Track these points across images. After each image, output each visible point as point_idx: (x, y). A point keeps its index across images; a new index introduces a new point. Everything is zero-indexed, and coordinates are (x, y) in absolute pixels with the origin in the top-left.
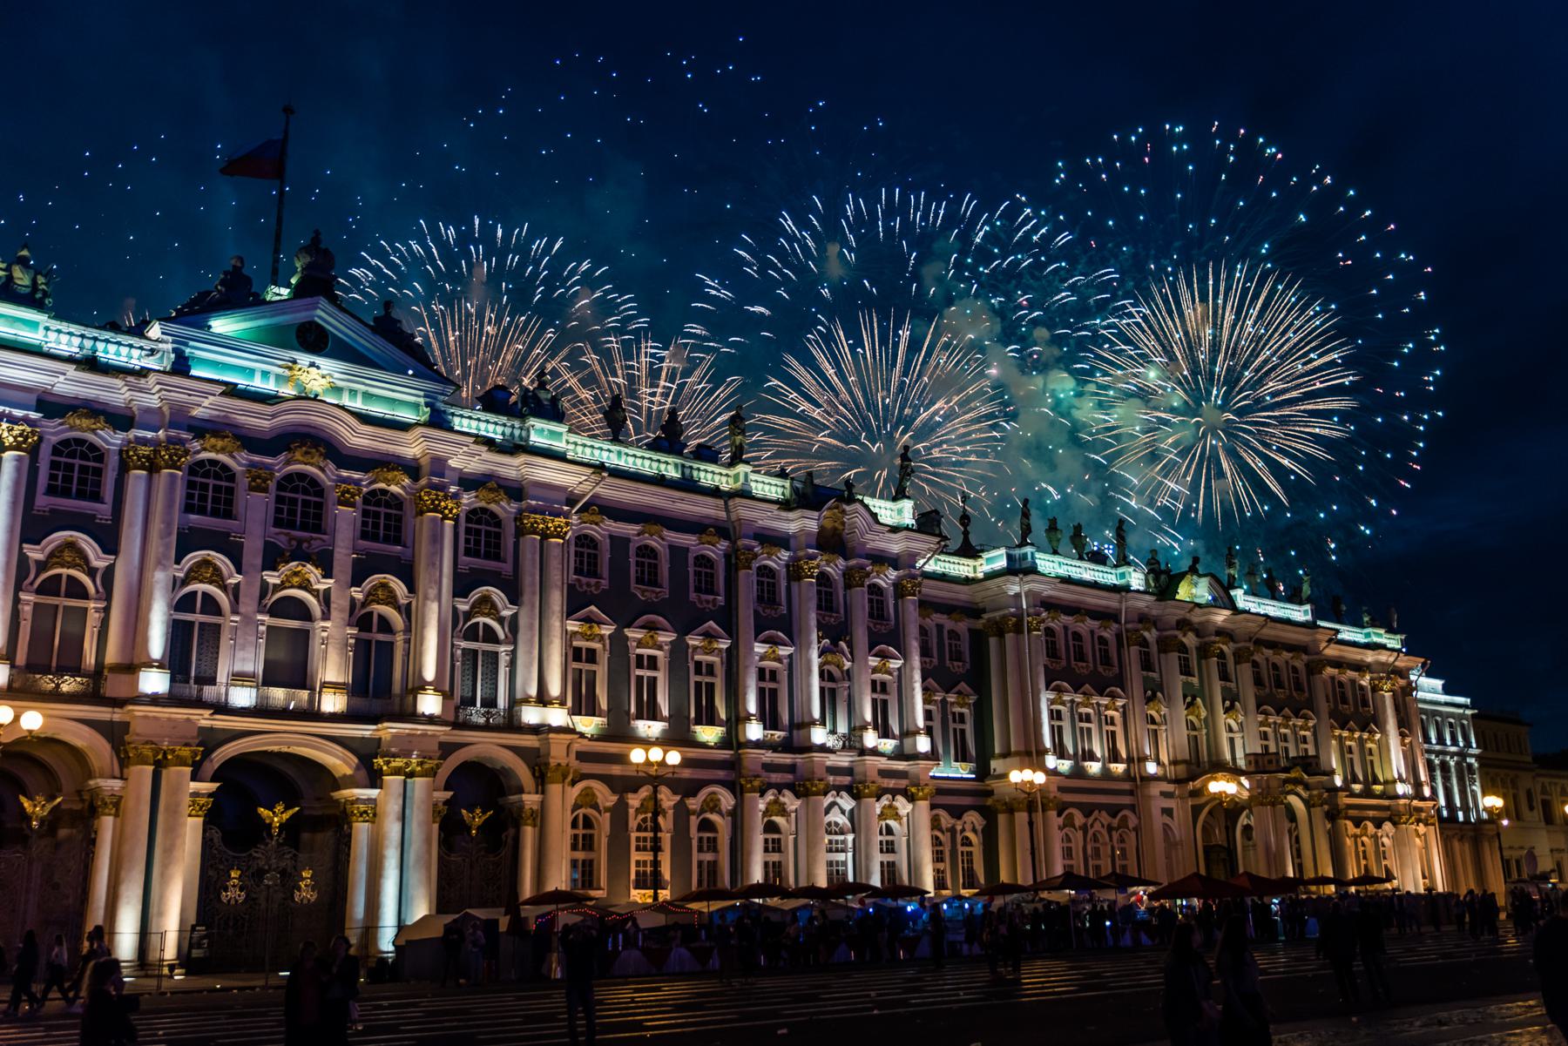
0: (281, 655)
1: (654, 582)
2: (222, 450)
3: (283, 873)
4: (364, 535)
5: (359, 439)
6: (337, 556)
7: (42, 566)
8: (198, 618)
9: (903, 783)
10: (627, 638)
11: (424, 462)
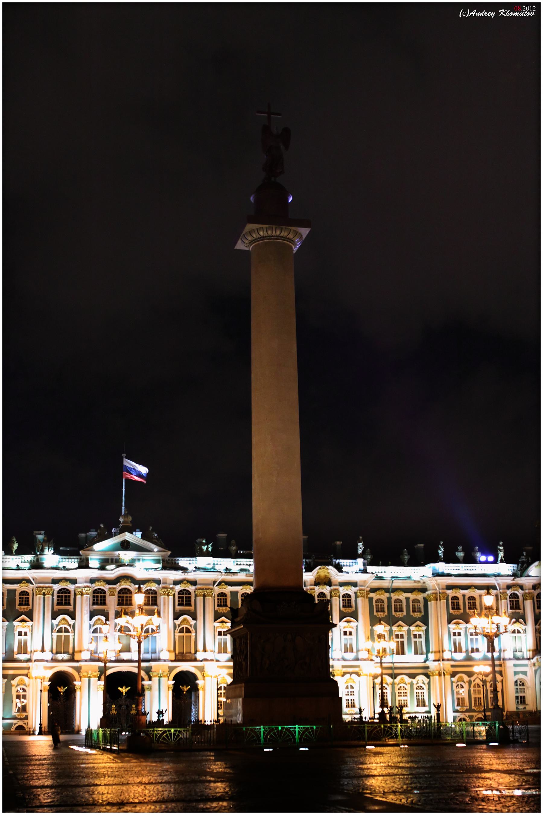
3: (127, 706)
7: (57, 625)
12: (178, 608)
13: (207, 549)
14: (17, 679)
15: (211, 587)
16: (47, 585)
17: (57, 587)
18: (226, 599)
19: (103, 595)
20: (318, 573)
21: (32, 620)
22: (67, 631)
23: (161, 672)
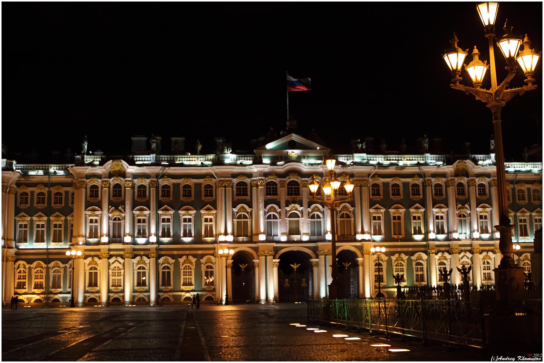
2: (273, 179)
7: (237, 213)
9: (492, 248)
11: (324, 172)
13: (362, 146)
14: (205, 258)
15: (366, 178)
16: (227, 179)
17: (235, 181)
18: (379, 189)
20: (457, 166)
21: (216, 209)
22: (245, 217)
23: (326, 251)
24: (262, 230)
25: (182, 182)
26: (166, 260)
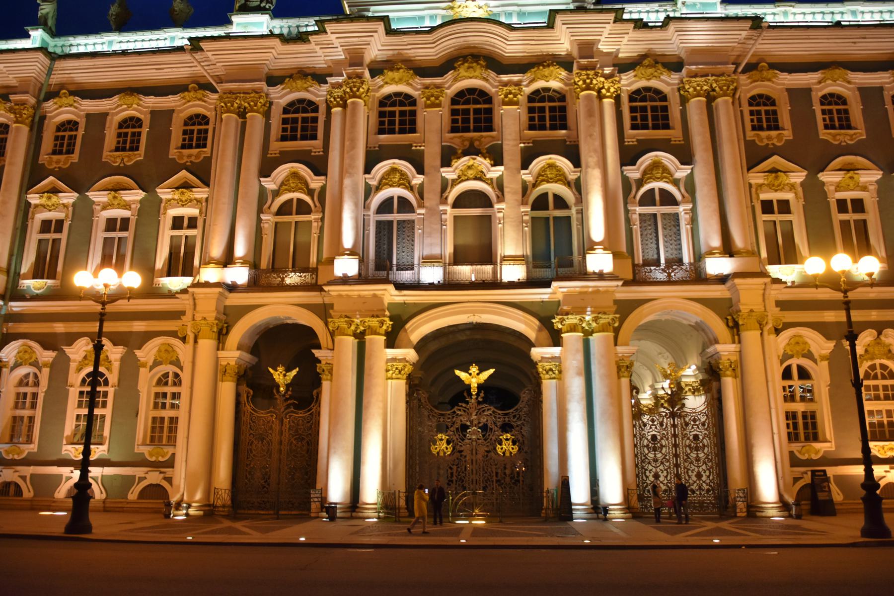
0: (469, 239)
1: (846, 124)
2: (400, 81)
4: (531, 128)
5: (512, 47)
6: (505, 147)
7: (276, 193)
8: (395, 217)
10: (823, 184)
11: (575, 53)
12: (632, 135)
16: (248, 86)
19: (407, 108)
21: (207, 184)
24: (348, 240)
25: (117, 109)
26: (28, 350)
